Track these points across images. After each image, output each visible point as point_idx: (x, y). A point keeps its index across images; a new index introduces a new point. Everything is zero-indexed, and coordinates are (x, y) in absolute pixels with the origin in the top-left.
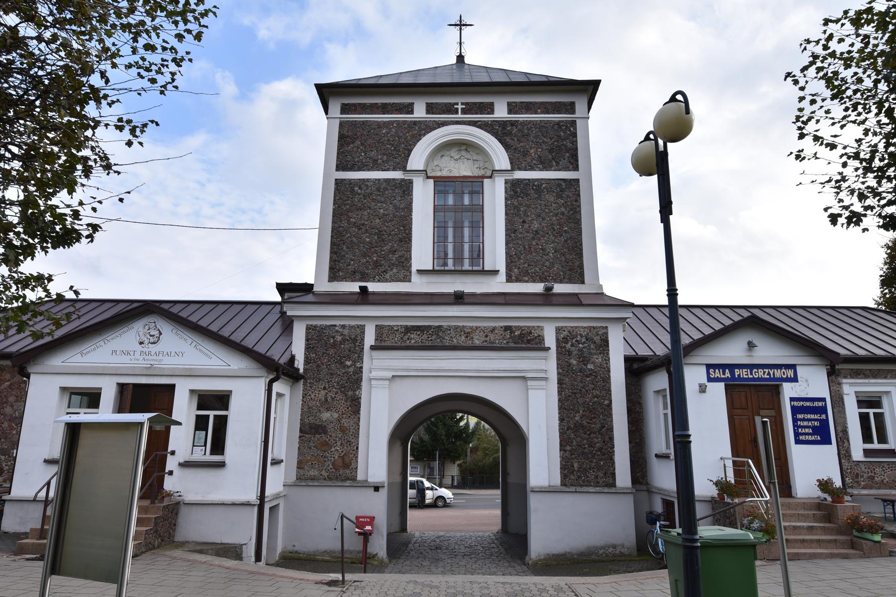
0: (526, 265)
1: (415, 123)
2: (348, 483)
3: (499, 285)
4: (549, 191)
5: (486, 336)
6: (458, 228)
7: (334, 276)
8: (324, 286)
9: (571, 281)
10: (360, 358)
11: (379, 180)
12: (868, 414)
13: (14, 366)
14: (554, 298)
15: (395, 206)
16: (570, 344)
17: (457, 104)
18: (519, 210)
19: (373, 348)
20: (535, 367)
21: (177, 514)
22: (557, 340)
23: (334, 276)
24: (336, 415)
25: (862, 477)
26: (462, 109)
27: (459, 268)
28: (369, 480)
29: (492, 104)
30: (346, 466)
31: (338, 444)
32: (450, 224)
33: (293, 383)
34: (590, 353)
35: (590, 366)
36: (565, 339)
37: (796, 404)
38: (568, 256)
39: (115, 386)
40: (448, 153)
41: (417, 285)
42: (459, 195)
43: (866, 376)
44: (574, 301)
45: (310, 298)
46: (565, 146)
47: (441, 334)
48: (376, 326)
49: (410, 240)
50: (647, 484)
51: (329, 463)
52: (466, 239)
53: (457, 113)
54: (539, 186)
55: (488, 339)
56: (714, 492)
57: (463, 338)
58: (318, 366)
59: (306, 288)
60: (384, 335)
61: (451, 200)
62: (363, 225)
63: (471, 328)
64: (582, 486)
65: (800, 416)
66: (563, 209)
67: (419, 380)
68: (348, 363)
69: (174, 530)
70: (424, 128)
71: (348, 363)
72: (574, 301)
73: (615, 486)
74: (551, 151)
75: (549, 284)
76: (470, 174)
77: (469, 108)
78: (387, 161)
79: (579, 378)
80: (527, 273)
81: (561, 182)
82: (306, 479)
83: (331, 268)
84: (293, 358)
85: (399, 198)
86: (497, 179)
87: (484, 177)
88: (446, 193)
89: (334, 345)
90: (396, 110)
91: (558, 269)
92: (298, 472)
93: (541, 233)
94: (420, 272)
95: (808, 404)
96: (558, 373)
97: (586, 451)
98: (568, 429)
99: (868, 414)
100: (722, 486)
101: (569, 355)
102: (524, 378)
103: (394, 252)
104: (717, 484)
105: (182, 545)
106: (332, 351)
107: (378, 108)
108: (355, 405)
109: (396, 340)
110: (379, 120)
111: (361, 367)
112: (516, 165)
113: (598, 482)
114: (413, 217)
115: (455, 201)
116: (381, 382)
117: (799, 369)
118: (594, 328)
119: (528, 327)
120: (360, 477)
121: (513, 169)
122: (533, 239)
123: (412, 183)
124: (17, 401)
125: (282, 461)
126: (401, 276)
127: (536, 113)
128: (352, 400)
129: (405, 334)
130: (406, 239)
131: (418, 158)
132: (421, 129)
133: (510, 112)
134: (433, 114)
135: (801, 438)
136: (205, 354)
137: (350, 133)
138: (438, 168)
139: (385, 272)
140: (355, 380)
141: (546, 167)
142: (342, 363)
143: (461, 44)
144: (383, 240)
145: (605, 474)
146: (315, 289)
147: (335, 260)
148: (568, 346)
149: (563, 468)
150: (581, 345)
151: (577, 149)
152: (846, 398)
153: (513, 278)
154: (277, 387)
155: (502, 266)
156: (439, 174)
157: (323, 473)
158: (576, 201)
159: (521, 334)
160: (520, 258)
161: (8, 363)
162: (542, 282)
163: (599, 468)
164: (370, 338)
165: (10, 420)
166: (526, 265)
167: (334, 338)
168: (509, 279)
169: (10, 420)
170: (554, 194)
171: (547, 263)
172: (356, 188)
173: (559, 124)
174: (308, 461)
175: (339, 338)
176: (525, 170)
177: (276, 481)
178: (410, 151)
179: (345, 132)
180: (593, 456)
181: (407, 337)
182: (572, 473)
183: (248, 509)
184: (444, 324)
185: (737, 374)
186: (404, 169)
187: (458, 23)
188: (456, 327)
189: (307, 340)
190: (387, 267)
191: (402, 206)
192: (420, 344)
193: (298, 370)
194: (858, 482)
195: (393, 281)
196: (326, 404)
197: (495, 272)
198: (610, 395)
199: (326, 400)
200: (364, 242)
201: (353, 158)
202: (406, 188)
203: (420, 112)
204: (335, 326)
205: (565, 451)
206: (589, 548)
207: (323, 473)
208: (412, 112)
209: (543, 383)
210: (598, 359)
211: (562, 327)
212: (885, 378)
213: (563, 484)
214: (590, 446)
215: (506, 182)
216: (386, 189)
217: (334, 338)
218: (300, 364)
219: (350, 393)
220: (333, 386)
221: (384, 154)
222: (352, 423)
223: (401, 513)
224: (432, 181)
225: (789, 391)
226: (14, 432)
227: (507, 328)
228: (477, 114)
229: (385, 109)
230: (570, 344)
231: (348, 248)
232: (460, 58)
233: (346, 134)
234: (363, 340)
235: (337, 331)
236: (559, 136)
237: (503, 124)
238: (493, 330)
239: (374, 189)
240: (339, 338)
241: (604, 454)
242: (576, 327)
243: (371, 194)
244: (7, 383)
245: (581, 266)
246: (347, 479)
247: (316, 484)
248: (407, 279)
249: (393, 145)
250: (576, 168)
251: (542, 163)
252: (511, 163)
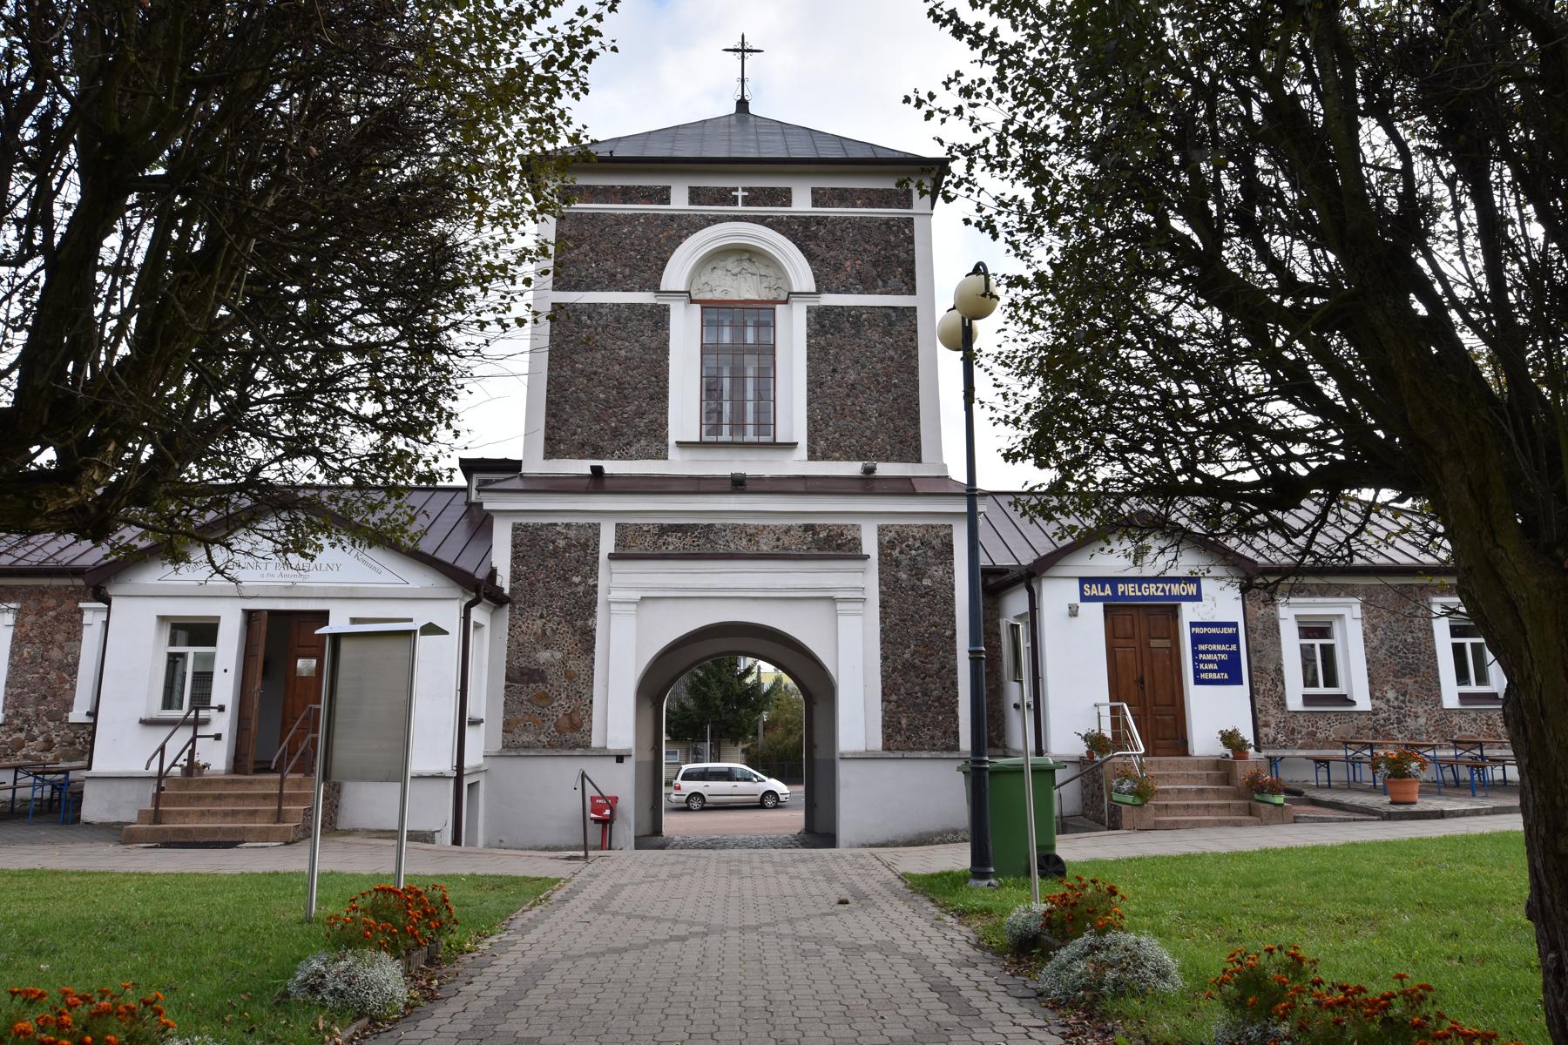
0: (837, 435)
1: (672, 218)
2: (578, 752)
3: (797, 464)
4: (873, 324)
5: (778, 539)
7: (551, 451)
8: (536, 465)
9: (902, 458)
10: (594, 573)
11: (619, 305)
12: (1313, 646)
13: (88, 586)
14: (876, 484)
15: (643, 346)
16: (898, 550)
17: (736, 189)
18: (827, 353)
19: (612, 557)
20: (847, 584)
21: (339, 792)
22: (880, 544)
23: (551, 451)
24: (558, 655)
25: (1299, 732)
26: (744, 197)
27: (738, 439)
28: (609, 747)
29: (789, 191)
30: (575, 727)
31: (563, 696)
32: (726, 372)
33: (495, 609)
34: (928, 564)
35: (926, 582)
36: (890, 544)
37: (1197, 630)
38: (898, 422)
39: (240, 613)
40: (722, 264)
41: (677, 464)
42: (738, 328)
43: (1312, 594)
44: (905, 488)
45: (517, 484)
46: (897, 256)
47: (711, 536)
48: (617, 525)
49: (666, 397)
50: (1005, 746)
51: (549, 723)
52: (750, 394)
53: (736, 203)
54: (858, 317)
55: (780, 543)
56: (1081, 749)
57: (744, 542)
58: (531, 584)
59: (510, 467)
60: (629, 539)
61: (726, 337)
62: (595, 373)
63: (756, 527)
64: (911, 750)
65: (1202, 647)
66: (892, 352)
67: (681, 605)
68: (576, 579)
69: (336, 814)
70: (689, 225)
71: (576, 579)
72: (905, 488)
73: (958, 750)
74: (875, 264)
75: (869, 464)
76: (756, 298)
77: (754, 197)
78: (631, 277)
79: (910, 600)
80: (838, 447)
81: (890, 311)
82: (516, 748)
83: (548, 439)
84: (493, 573)
85: (650, 334)
86: (795, 306)
87: (776, 302)
88: (719, 325)
89: (554, 554)
90: (643, 197)
91: (883, 440)
92: (504, 737)
93: (859, 387)
94: (681, 445)
95: (1214, 630)
96: (881, 592)
97: (918, 701)
98: (893, 671)
99: (1313, 646)
100: (1095, 742)
101: (897, 566)
102: (832, 599)
103: (642, 415)
104: (1086, 738)
105: (352, 832)
106: (551, 562)
107: (615, 194)
108: (586, 640)
109: (646, 545)
110: (618, 212)
111: (596, 586)
112: (823, 286)
113: (934, 745)
114: (670, 362)
115: (733, 337)
116: (624, 607)
117: (1204, 582)
118: (933, 527)
119: (839, 526)
120: (596, 742)
121: (819, 291)
122: (848, 396)
123: (668, 310)
124: (68, 640)
125: (482, 721)
126: (653, 451)
127: (854, 206)
128: (583, 633)
129: (660, 537)
130: (659, 395)
131: (676, 273)
132: (681, 228)
133: (816, 203)
134: (700, 204)
135: (1203, 676)
136: (371, 567)
137: (573, 232)
138: (708, 288)
139: (629, 444)
140: (586, 604)
141: (868, 289)
142: (566, 579)
143: (743, 81)
144: (626, 397)
145: (945, 733)
146: (524, 470)
147: (553, 427)
148: (896, 553)
149: (885, 726)
150: (913, 552)
151: (913, 262)
152: (1282, 624)
153: (819, 454)
154: (477, 614)
155: (801, 437)
156: (708, 296)
157: (542, 738)
158: (912, 340)
159: (828, 536)
160: (827, 425)
161: (80, 582)
162: (860, 459)
163: (936, 725)
164: (607, 544)
165: (58, 669)
166: (837, 435)
167: (554, 542)
168: (812, 456)
169: (58, 669)
170: (880, 330)
171: (868, 433)
172: (584, 318)
173: (887, 222)
174: (518, 722)
175: (561, 543)
176: (838, 292)
177: (478, 746)
178: (665, 261)
179: (566, 230)
180: (929, 709)
181: (662, 541)
182: (899, 732)
183: (442, 783)
184: (717, 521)
185: (1120, 591)
186: (655, 288)
187: (740, 47)
188: (735, 527)
189: (514, 546)
190: (631, 438)
191: (653, 346)
192: (682, 551)
193: (502, 589)
194: (1293, 740)
195: (641, 458)
196: (544, 640)
198: (954, 622)
199: (544, 633)
200: (597, 400)
201: (579, 271)
202: (658, 318)
203: (679, 201)
204: (556, 525)
205: (890, 702)
206: (920, 834)
207: (542, 738)
208: (667, 201)
209: (860, 606)
210: (938, 572)
211: (887, 526)
212: (1338, 596)
213: (886, 748)
214: (925, 694)
215: (809, 310)
216: (629, 319)
217: (554, 542)
218: (504, 581)
219: (579, 623)
220: (554, 613)
221: (625, 266)
222: (582, 665)
223: (652, 808)
224: (698, 307)
225: (1189, 613)
226: (67, 686)
227: (808, 528)
228: (765, 205)
229: (626, 195)
230: (898, 550)
231: (572, 407)
232: (742, 105)
233: (568, 233)
234: (597, 545)
235: (559, 533)
236: (888, 242)
237: (805, 221)
238: (788, 530)
239: (610, 318)
240: (561, 543)
241: (943, 706)
242: (907, 526)
243: (607, 326)
244: (52, 613)
245: (917, 437)
246: (577, 746)
247: (532, 753)
248: (662, 454)
249: (638, 252)
250: (912, 291)
251: (862, 282)
252: (816, 282)
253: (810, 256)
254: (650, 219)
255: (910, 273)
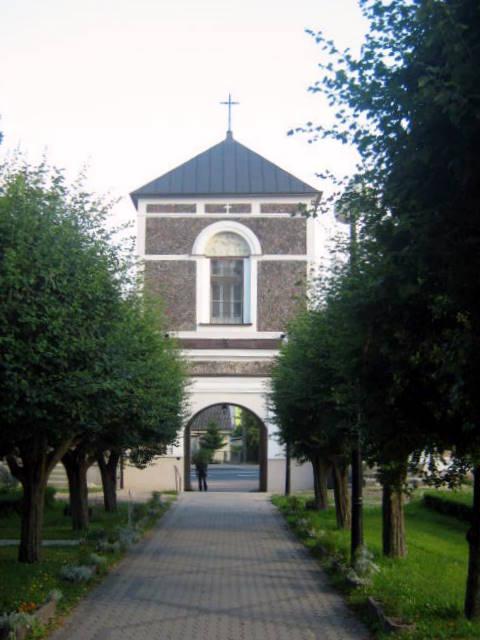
3: (251, 333)
6: (227, 295)
41: (201, 333)
53: (225, 211)
54: (280, 266)
70: (206, 222)
77: (234, 209)
80: (270, 325)
87: (243, 257)
103: (185, 311)
112: (265, 251)
139: (179, 325)
141: (286, 252)
155: (254, 319)
168: (259, 329)
178: (194, 240)
184: (218, 360)
197: (250, 324)
202: (191, 267)
215: (258, 263)
227: (257, 363)
229: (177, 209)
232: (229, 133)
237: (257, 220)
238: (247, 364)
253: (260, 237)
254: (187, 221)
255: (304, 244)
